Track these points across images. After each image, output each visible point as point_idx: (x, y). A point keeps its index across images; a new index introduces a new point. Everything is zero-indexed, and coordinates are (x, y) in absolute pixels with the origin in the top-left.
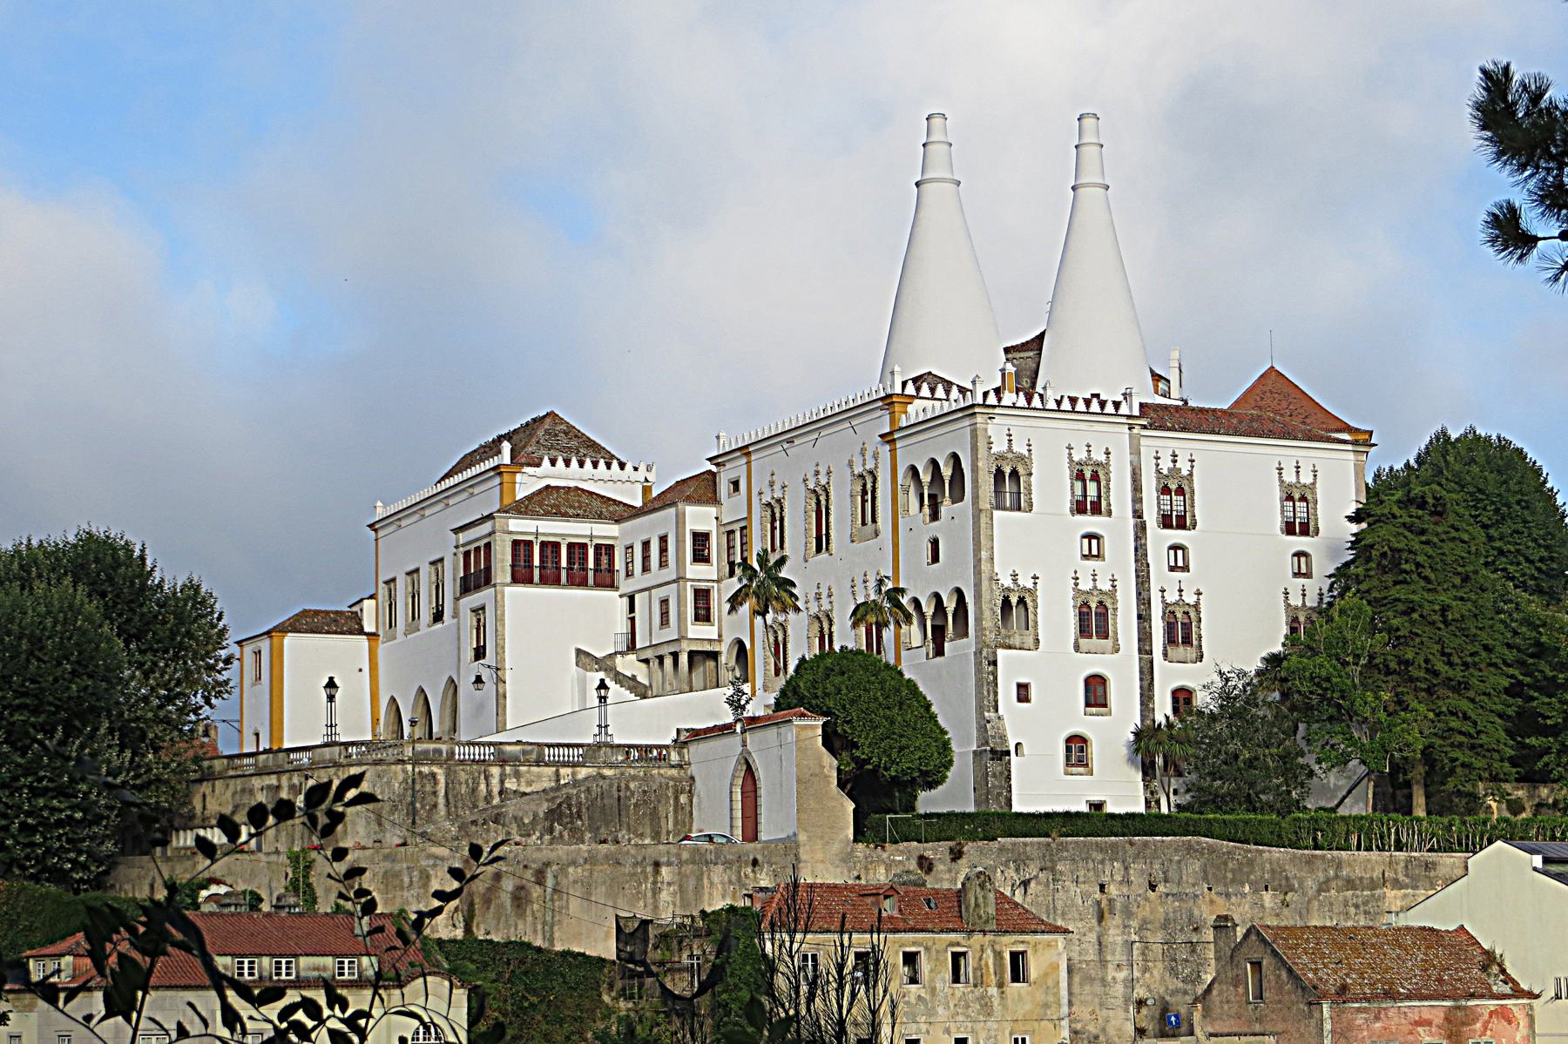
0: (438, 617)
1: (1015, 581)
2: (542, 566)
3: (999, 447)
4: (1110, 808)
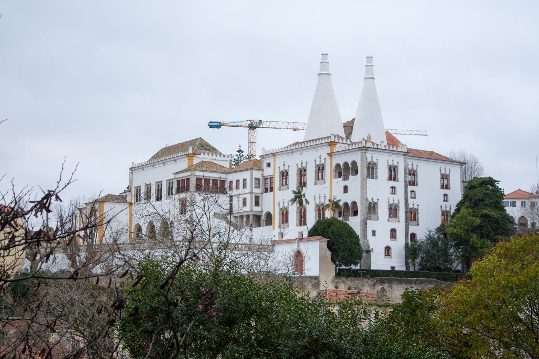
2: (203, 186)
3: (369, 160)
4: (396, 269)
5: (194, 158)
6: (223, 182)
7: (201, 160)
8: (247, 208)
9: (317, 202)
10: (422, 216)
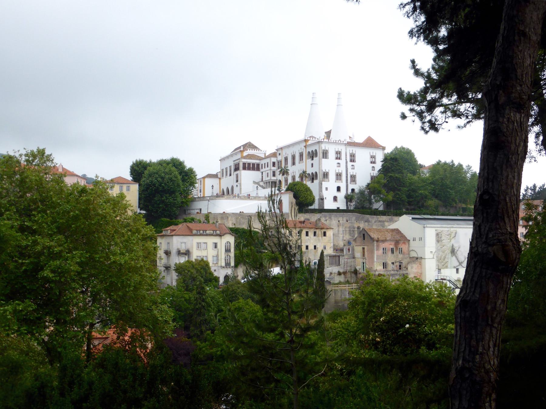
0: (230, 175)
2: (247, 167)
3: (323, 148)
6: (258, 165)
8: (269, 178)
10: (358, 179)
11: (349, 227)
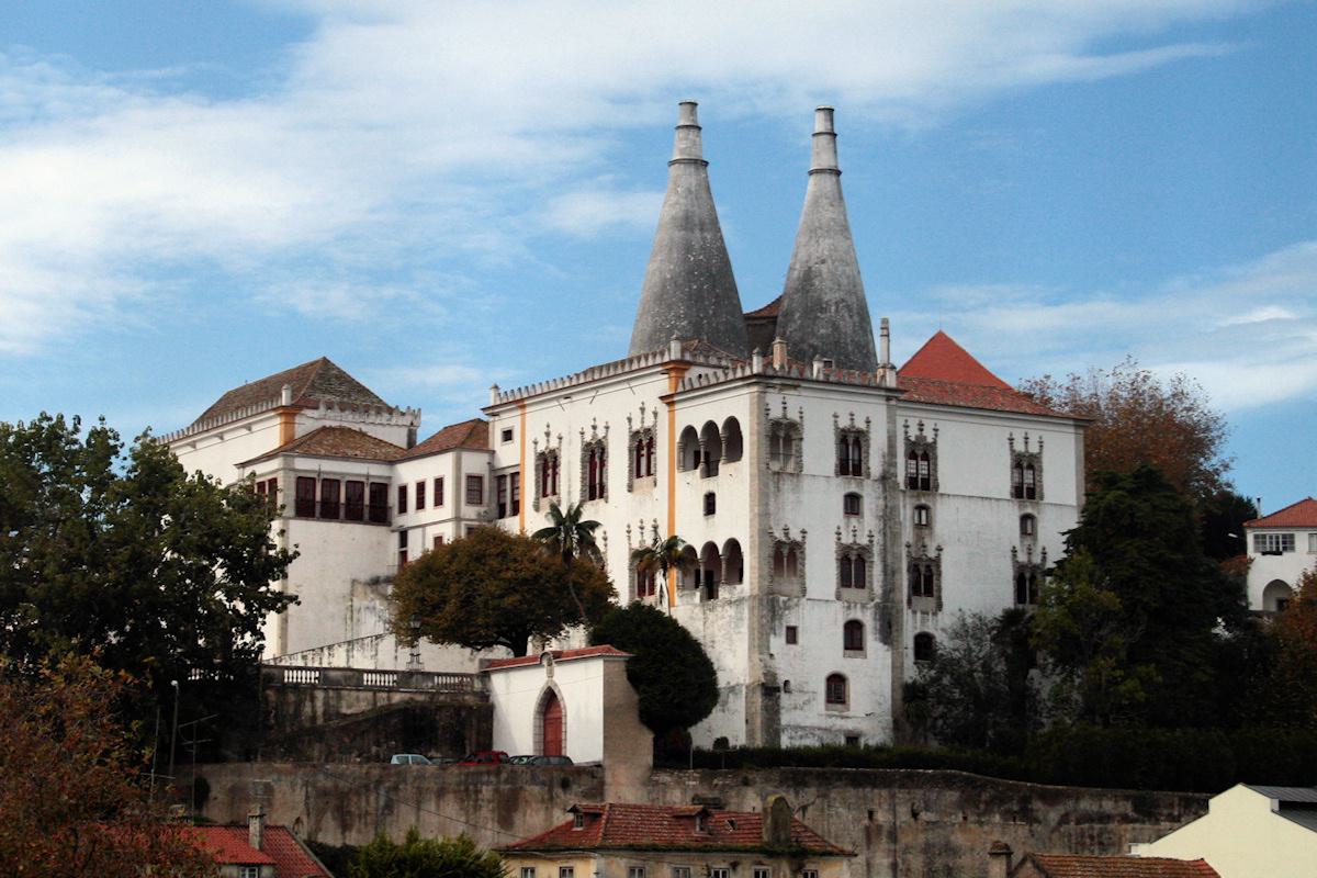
1: (787, 534)
2: (319, 502)
3: (776, 413)
5: (298, 419)
6: (380, 490)
7: (319, 425)
9: (636, 546)
11: (927, 849)
